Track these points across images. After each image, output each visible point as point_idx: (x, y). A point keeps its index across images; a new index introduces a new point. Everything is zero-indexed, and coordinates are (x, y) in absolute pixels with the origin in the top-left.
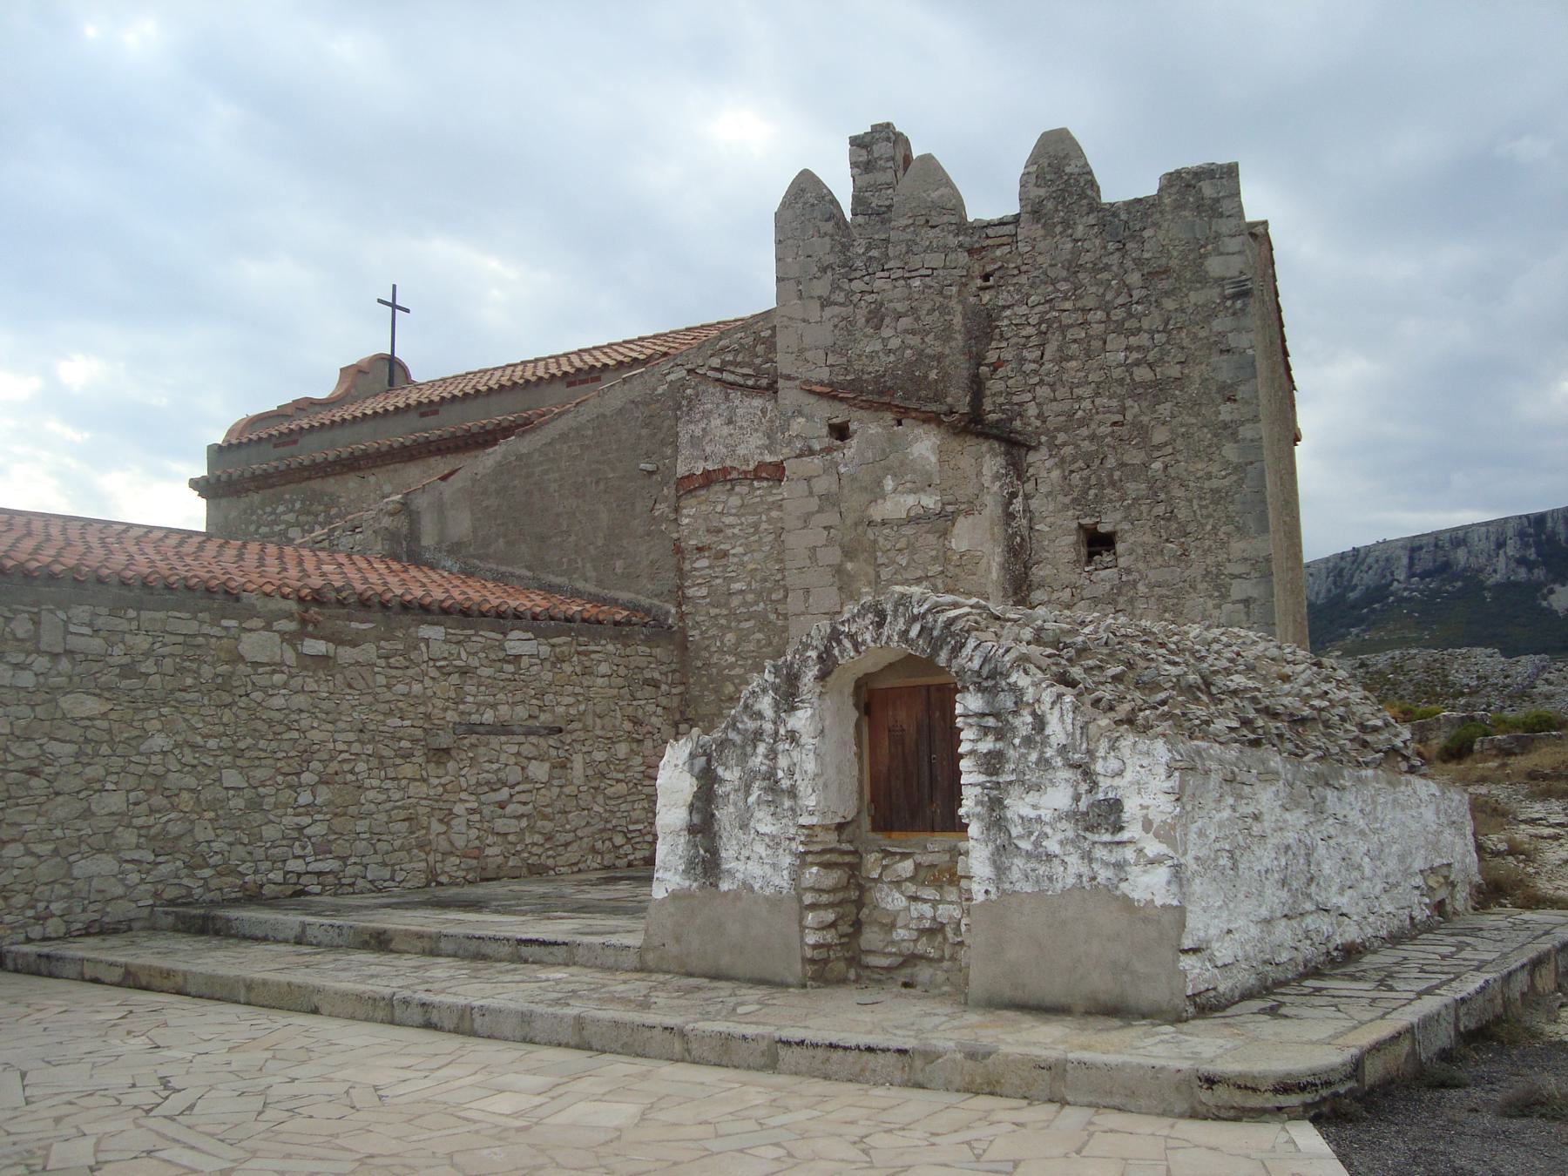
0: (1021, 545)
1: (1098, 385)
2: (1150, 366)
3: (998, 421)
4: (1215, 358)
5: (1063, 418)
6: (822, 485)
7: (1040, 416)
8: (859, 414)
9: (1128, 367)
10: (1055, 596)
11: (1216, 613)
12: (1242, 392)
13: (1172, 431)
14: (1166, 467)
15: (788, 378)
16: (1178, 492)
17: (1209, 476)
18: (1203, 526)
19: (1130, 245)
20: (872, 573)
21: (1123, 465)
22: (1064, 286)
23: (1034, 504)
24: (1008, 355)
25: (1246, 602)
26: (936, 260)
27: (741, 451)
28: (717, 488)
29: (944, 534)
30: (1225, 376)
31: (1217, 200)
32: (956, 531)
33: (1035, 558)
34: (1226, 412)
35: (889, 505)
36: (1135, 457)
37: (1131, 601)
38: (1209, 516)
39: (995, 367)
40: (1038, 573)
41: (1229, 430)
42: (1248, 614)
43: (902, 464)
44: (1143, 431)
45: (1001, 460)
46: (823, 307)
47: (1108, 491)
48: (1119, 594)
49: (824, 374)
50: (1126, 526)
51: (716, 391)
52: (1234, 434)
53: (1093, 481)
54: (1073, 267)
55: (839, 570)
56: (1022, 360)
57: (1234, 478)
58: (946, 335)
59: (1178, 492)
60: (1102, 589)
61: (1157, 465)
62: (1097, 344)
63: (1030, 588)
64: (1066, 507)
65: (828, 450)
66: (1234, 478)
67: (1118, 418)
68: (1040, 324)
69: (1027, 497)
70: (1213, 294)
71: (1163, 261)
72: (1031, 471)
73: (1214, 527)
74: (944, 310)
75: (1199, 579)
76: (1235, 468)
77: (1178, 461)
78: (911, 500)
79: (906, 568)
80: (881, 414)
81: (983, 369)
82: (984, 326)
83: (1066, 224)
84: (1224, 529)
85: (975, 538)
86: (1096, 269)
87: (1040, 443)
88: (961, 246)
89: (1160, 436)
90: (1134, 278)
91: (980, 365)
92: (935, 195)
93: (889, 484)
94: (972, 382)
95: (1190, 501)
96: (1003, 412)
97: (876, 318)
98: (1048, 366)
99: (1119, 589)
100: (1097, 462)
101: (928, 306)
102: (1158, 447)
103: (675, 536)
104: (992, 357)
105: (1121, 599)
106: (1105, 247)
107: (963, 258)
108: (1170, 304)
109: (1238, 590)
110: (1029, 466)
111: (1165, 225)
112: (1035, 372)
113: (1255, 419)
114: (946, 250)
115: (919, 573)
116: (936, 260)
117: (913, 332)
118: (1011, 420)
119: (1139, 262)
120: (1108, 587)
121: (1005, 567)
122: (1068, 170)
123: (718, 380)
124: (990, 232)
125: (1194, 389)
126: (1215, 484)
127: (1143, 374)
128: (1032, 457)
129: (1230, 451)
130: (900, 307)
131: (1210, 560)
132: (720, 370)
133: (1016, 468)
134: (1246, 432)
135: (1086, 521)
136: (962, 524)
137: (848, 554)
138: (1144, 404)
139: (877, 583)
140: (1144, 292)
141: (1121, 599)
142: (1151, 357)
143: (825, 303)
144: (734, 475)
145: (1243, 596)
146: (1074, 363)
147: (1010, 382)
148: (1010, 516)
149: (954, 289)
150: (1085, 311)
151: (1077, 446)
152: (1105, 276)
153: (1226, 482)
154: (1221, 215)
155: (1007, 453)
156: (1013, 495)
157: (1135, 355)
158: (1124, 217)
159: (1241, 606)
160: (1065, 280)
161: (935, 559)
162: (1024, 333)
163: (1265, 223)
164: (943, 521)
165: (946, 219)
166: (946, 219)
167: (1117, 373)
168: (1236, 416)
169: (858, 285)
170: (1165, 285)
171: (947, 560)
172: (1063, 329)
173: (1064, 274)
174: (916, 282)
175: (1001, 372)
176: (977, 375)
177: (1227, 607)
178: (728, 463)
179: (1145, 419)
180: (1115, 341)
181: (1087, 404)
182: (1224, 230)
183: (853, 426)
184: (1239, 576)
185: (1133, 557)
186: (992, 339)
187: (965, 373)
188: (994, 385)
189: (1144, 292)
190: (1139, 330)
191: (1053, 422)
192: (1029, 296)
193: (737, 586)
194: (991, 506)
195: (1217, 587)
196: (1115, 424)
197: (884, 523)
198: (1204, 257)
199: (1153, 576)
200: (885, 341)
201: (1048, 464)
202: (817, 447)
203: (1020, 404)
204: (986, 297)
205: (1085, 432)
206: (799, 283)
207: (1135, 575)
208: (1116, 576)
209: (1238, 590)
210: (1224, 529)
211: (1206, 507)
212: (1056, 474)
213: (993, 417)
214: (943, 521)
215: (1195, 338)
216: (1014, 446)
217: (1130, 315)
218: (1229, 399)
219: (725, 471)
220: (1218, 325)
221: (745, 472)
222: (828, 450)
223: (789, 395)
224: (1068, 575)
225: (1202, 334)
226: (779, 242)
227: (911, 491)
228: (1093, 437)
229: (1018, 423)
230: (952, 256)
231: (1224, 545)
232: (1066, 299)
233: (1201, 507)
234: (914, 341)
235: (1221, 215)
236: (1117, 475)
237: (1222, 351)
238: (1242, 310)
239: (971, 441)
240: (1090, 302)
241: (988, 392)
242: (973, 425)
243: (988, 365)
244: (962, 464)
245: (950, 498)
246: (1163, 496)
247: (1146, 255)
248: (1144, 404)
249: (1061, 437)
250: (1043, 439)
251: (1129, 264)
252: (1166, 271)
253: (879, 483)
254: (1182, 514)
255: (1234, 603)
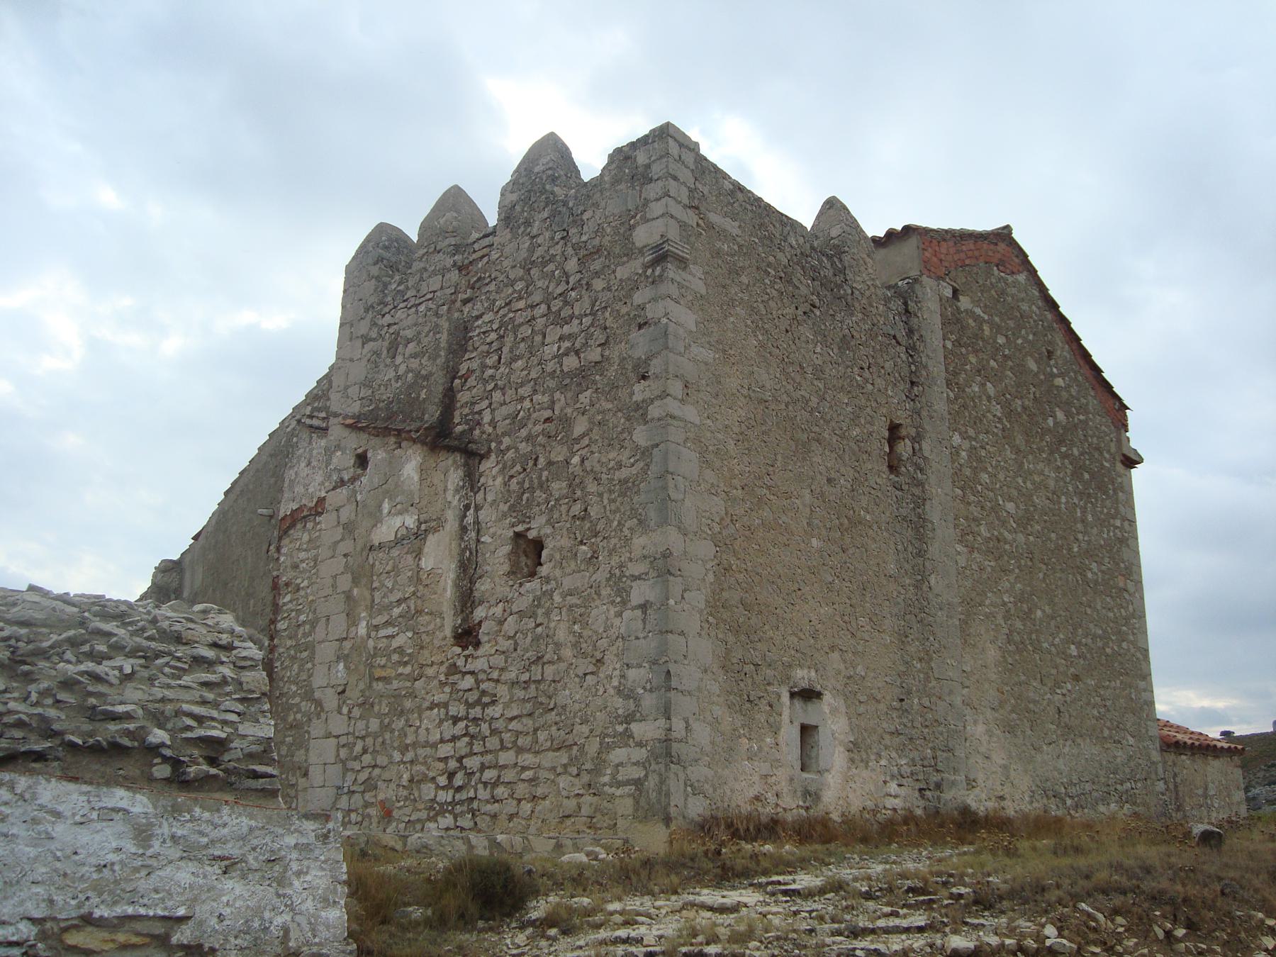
0: (469, 560)
1: (535, 380)
2: (577, 353)
3: (463, 432)
4: (635, 335)
5: (508, 421)
6: (346, 514)
7: (493, 423)
8: (376, 441)
9: (559, 357)
10: (490, 613)
11: (617, 622)
12: (656, 366)
13: (591, 421)
14: (583, 461)
15: (336, 415)
16: (592, 487)
17: (620, 466)
18: (610, 521)
19: (573, 231)
20: (369, 597)
21: (550, 463)
22: (519, 286)
23: (482, 515)
24: (475, 365)
25: (644, 607)
26: (435, 283)
27: (311, 490)
28: (299, 526)
29: (418, 555)
30: (640, 353)
31: (648, 166)
32: (426, 550)
33: (479, 571)
34: (640, 391)
35: (384, 528)
36: (559, 453)
37: (547, 614)
38: (618, 510)
39: (465, 378)
40: (482, 587)
41: (639, 412)
42: (644, 621)
43: (397, 485)
44: (567, 422)
45: (460, 473)
46: (363, 344)
47: (538, 493)
48: (538, 606)
49: (356, 408)
50: (548, 530)
51: (305, 435)
52: (644, 415)
53: (526, 485)
54: (527, 266)
55: (348, 596)
56: (484, 367)
57: (641, 464)
58: (433, 358)
59: (592, 487)
60: (522, 604)
61: (576, 460)
62: (538, 338)
63: (473, 606)
64: (504, 516)
65: (353, 480)
66: (641, 464)
67: (548, 414)
68: (500, 328)
69: (478, 508)
70: (636, 265)
71: (597, 242)
72: (482, 480)
73: (619, 523)
74: (436, 329)
75: (604, 583)
76: (643, 453)
77: (592, 453)
78: (397, 521)
79: (391, 591)
80: (386, 439)
81: (457, 381)
82: (461, 339)
83: (528, 223)
84: (629, 524)
85: (439, 556)
86: (544, 264)
87: (490, 450)
88: (455, 264)
89: (580, 427)
90: (572, 265)
91: (454, 378)
92: (442, 221)
93: (386, 506)
94: (445, 396)
95: (601, 495)
96: (467, 423)
97: (393, 350)
98: (502, 370)
99: (539, 599)
100: (531, 463)
101: (427, 329)
102: (577, 440)
103: (275, 573)
104: (463, 369)
105: (540, 611)
106: (552, 238)
107: (454, 276)
108: (598, 284)
109: (639, 593)
110: (480, 476)
111: (602, 204)
112: (492, 377)
113: (664, 395)
114: (444, 271)
115: (399, 595)
116: (435, 283)
117: (414, 356)
118: (472, 430)
119: (576, 247)
120: (531, 598)
121: (457, 585)
122: (536, 170)
123: (311, 426)
124: (476, 246)
125: (612, 372)
126: (624, 473)
127: (571, 362)
128: (486, 465)
129: (641, 436)
130: (409, 333)
131: (615, 560)
132: (311, 417)
133: (472, 481)
134: (654, 411)
135: (520, 528)
136: (432, 539)
137: (356, 581)
138: (569, 395)
139: (372, 607)
140: (579, 276)
141: (540, 611)
142: (577, 345)
143: (366, 339)
144: (305, 513)
145: (642, 601)
146: (520, 362)
147: (475, 391)
148: (464, 529)
149: (445, 308)
150: (532, 307)
151: (517, 449)
152: (551, 267)
153: (634, 470)
154: (651, 180)
155: (466, 464)
156: (467, 507)
157: (567, 344)
158: (571, 205)
159: (638, 612)
160: (521, 279)
161: (410, 578)
162: (488, 340)
163: (1008, 227)
164: (416, 539)
165: (447, 242)
166: (447, 242)
167: (550, 367)
168: (647, 395)
169: (388, 319)
170: (596, 265)
171: (419, 580)
172: (515, 330)
173: (521, 272)
174: (422, 308)
175: (468, 384)
176: (451, 389)
177: (627, 614)
178: (304, 502)
179: (569, 410)
180: (553, 333)
181: (527, 404)
182: (652, 196)
183: (369, 455)
184: (638, 578)
185: (552, 564)
186: (466, 351)
187: (441, 389)
188: (463, 397)
189: (579, 276)
190: (572, 317)
191: (503, 426)
192: (495, 301)
193: (303, 618)
194: (452, 525)
195: (619, 592)
196: (547, 420)
197: (381, 546)
198: (632, 228)
199: (568, 583)
200: (397, 367)
201: (495, 471)
202: (346, 478)
203: (480, 413)
204: (466, 310)
205: (524, 433)
206: (352, 325)
207: (553, 584)
208: (538, 586)
209: (639, 593)
210: (629, 524)
211: (614, 501)
212: (499, 480)
213: (459, 429)
214: (416, 539)
215: (617, 315)
216: (471, 455)
217: (566, 303)
218: (644, 378)
219: (300, 509)
220: (638, 298)
221: (311, 509)
222: (353, 480)
223: (336, 431)
224: (503, 590)
225: (624, 310)
226: (345, 291)
227: (400, 513)
228: (528, 439)
229: (477, 432)
230: (447, 276)
231: (627, 540)
232: (520, 298)
233: (612, 501)
234: (414, 364)
235: (651, 180)
236: (545, 473)
237: (640, 327)
238: (660, 276)
239: (443, 455)
240: (537, 298)
241: (458, 405)
242: (442, 437)
243: (460, 378)
244: (436, 481)
245: (423, 517)
246: (579, 493)
247: (584, 238)
248: (569, 395)
249: (506, 441)
250: (493, 445)
251: (570, 251)
252: (598, 251)
253: (380, 506)
254: (593, 512)
255: (633, 609)
